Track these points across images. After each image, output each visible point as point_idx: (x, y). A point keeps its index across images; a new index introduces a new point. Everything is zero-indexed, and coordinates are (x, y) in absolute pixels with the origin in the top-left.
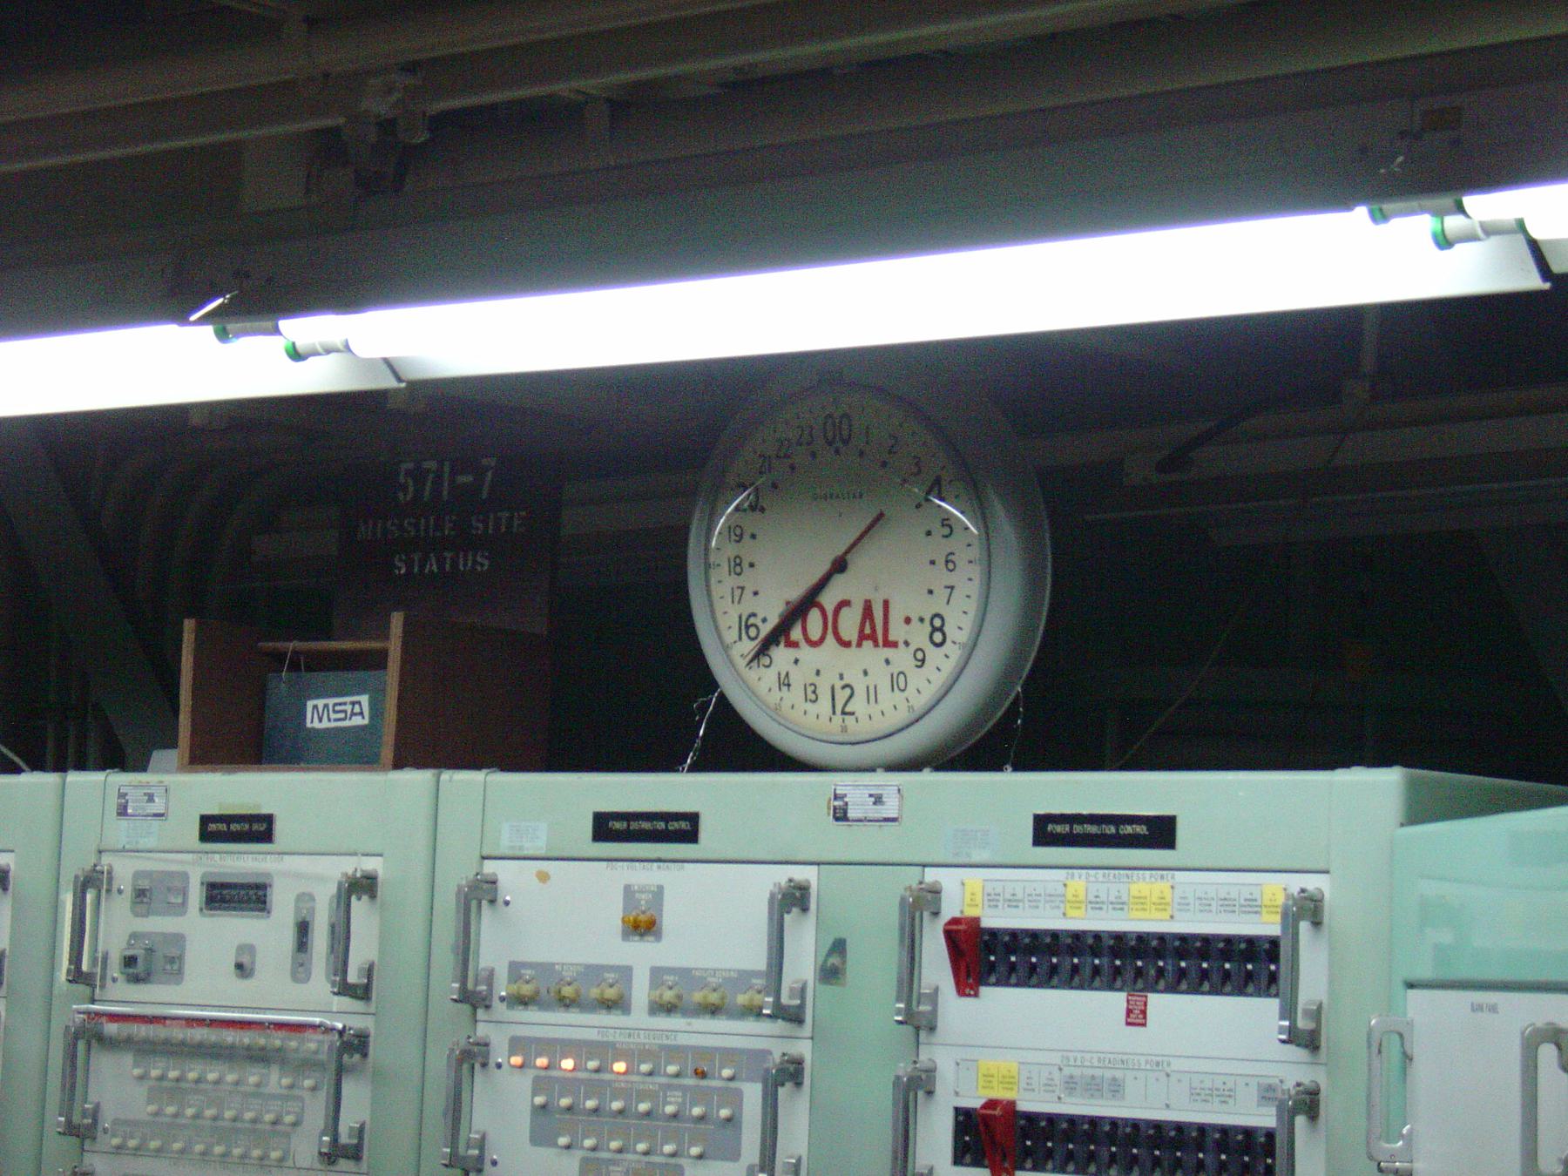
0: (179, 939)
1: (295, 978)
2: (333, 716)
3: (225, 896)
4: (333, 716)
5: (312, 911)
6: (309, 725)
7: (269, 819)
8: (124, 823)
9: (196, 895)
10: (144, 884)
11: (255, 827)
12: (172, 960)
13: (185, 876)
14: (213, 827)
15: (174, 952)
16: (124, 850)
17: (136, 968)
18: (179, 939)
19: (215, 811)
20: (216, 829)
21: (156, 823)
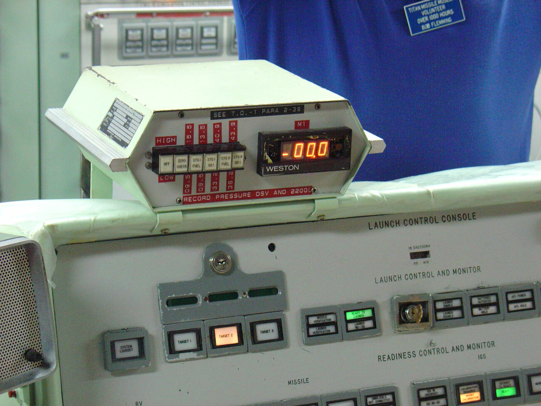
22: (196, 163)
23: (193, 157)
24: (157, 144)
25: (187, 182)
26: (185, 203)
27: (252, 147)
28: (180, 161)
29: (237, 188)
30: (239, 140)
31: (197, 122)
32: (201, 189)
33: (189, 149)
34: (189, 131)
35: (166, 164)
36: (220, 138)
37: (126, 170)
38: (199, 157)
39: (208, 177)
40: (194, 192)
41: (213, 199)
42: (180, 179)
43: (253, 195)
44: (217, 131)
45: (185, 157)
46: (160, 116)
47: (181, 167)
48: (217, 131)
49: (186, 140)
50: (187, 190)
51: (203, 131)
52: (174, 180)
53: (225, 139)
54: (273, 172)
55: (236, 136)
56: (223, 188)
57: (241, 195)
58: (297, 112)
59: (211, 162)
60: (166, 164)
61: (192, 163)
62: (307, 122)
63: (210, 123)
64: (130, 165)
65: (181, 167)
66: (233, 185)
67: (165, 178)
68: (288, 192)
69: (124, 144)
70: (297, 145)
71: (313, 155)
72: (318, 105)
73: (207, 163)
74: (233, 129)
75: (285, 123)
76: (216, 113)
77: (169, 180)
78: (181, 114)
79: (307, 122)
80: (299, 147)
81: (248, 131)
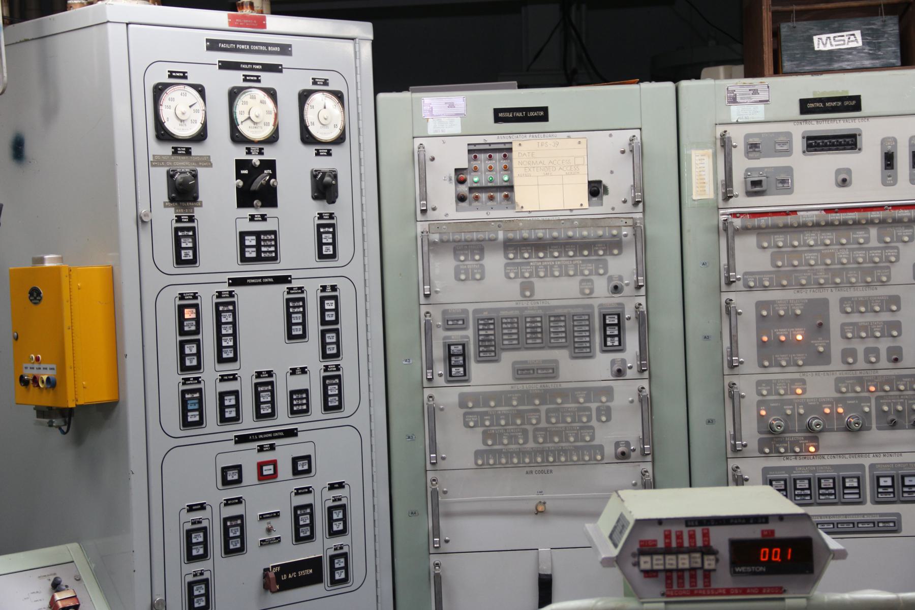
0: (789, 170)
1: (884, 183)
2: (834, 43)
3: (815, 144)
4: (834, 43)
5: (895, 146)
6: (816, 49)
7: (857, 98)
8: (734, 108)
9: (798, 144)
10: (752, 141)
11: (846, 103)
12: (783, 181)
13: (789, 135)
14: (811, 105)
15: (783, 177)
16: (737, 123)
17: (756, 187)
18: (789, 170)
19: (810, 96)
20: (807, 107)
21: (761, 107)
22: (671, 562)
23: (668, 557)
24: (641, 546)
25: (669, 579)
26: (668, 596)
27: (724, 551)
28: (657, 560)
29: (714, 586)
30: (712, 544)
31: (674, 529)
32: (681, 584)
33: (667, 551)
34: (667, 536)
35: (645, 562)
36: (695, 542)
37: (614, 566)
38: (674, 557)
39: (687, 575)
40: (675, 587)
41: (692, 593)
42: (662, 576)
43: (728, 592)
44: (692, 536)
45: (661, 557)
46: (640, 523)
47: (657, 565)
48: (692, 536)
49: (665, 543)
50: (669, 585)
51: (679, 536)
52: (656, 576)
53: (699, 543)
54: (741, 572)
55: (709, 541)
56: (700, 584)
57: (717, 592)
58: (762, 523)
59: (684, 562)
60: (646, 562)
61: (667, 562)
62: (772, 532)
63: (686, 531)
64: (617, 561)
65: (657, 565)
66: (709, 582)
67: (649, 574)
68: (760, 591)
69: (616, 546)
70: (763, 550)
71: (778, 559)
72: (781, 517)
73: (680, 562)
74: (706, 535)
75: (753, 532)
76: (690, 522)
77: (653, 576)
78: (660, 522)
79: (772, 532)
80: (765, 552)
81: (720, 538)
